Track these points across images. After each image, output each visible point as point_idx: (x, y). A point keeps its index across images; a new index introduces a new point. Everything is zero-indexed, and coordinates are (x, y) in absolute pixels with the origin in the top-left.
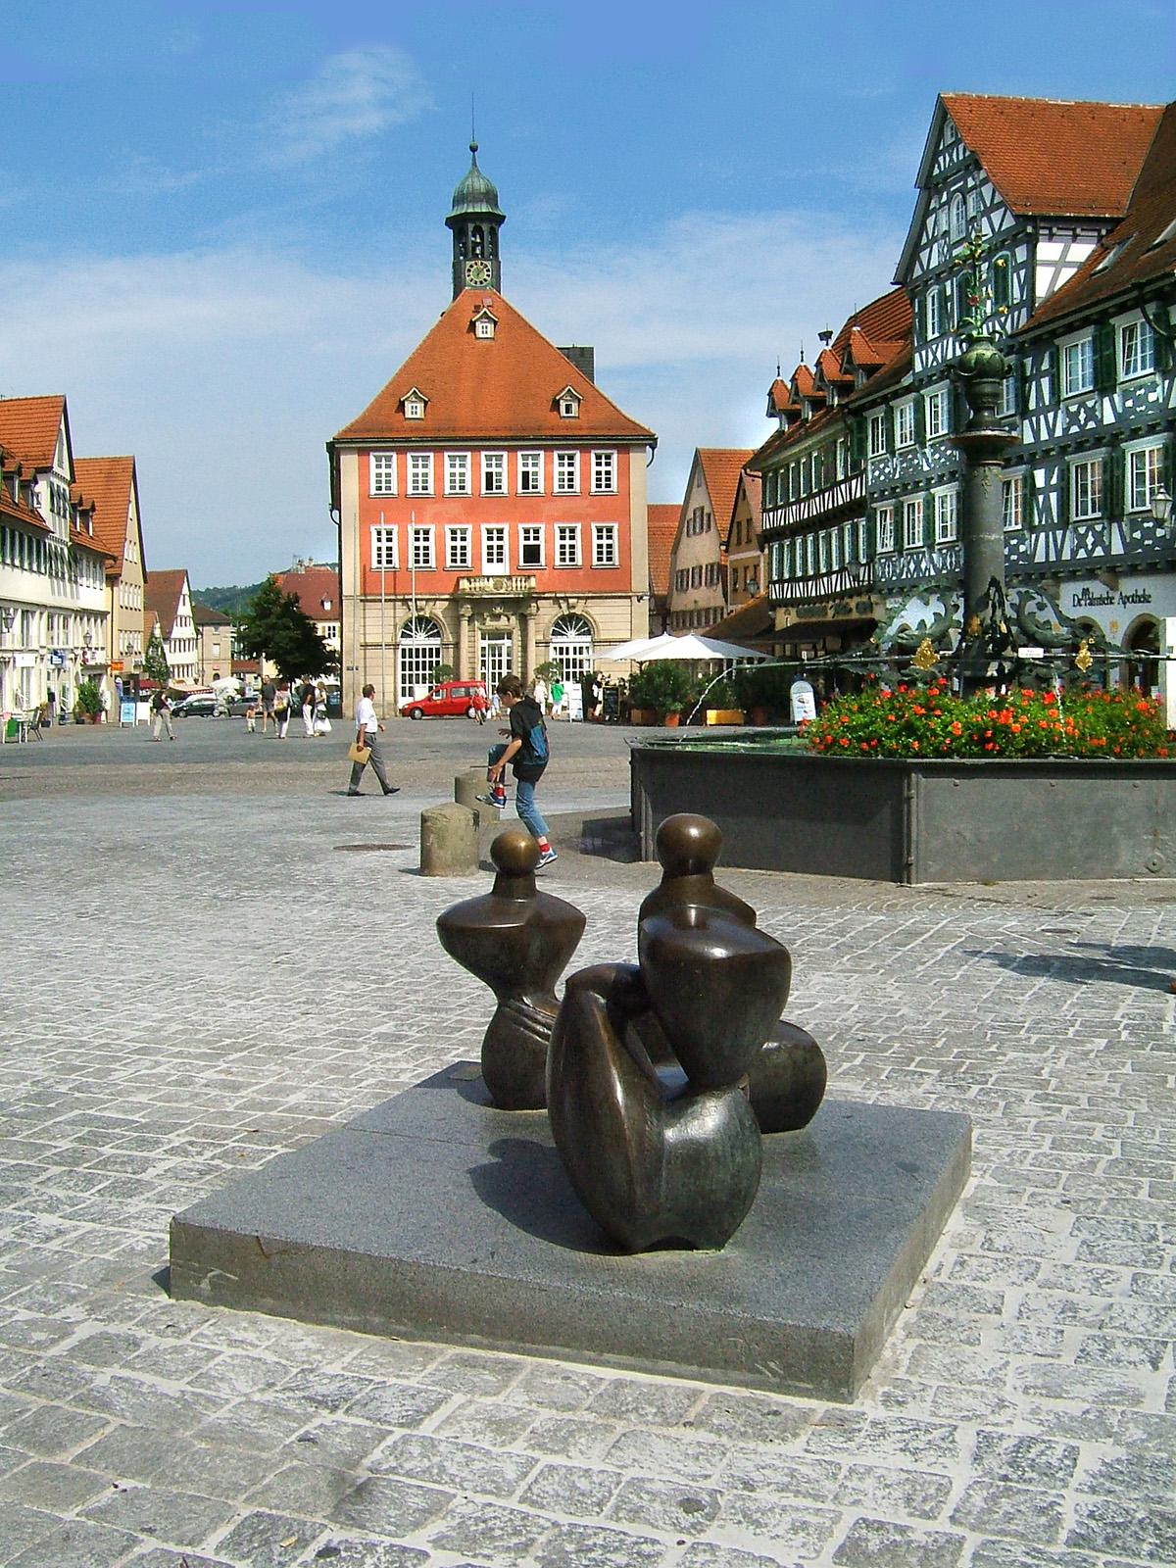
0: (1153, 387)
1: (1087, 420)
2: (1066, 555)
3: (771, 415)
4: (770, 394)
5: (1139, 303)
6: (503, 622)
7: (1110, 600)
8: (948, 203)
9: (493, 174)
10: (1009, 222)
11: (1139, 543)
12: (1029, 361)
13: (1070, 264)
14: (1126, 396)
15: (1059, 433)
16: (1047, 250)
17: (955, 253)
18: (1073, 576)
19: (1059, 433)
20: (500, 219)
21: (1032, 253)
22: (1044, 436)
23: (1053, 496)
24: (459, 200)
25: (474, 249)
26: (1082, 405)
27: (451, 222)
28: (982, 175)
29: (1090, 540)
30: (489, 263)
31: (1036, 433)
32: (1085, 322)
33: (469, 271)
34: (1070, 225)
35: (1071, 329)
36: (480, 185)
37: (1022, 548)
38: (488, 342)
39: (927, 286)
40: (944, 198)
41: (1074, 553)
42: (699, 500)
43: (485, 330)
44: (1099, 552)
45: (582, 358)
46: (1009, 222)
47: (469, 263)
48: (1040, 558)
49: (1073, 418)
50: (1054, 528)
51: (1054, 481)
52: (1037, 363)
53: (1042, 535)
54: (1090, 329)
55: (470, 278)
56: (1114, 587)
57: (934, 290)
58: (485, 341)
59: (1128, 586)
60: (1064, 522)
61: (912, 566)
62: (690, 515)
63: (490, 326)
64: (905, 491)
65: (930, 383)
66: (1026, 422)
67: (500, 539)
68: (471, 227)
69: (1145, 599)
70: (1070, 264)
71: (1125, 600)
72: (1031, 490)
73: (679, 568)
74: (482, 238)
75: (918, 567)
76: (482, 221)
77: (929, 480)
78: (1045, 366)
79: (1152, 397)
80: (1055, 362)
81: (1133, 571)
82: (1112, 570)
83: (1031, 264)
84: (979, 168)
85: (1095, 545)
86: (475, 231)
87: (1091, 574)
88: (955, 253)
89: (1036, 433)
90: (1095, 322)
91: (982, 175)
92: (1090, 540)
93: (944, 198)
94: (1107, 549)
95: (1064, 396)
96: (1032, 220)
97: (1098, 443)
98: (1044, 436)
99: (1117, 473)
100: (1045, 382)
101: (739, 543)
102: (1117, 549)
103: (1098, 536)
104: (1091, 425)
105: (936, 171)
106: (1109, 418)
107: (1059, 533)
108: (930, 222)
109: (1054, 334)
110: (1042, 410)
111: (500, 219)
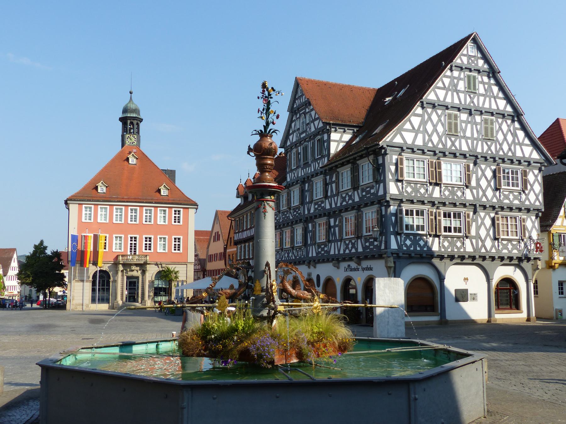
0: (372, 187)
1: (349, 200)
2: (342, 252)
3: (238, 197)
4: (237, 189)
5: (367, 155)
6: (135, 274)
7: (358, 269)
8: (299, 118)
9: (138, 103)
10: (321, 125)
11: (368, 247)
12: (328, 177)
13: (343, 142)
14: (363, 190)
15: (339, 205)
16: (335, 136)
17: (302, 136)
18: (344, 260)
19: (339, 205)
20: (141, 120)
21: (329, 136)
22: (333, 206)
23: (337, 229)
24: (125, 111)
25: (130, 130)
26: (347, 194)
27: (121, 119)
28: (311, 107)
29: (350, 246)
30: (136, 136)
31: (331, 205)
32: (348, 162)
34: (344, 126)
35: (343, 165)
36: (132, 106)
37: (326, 249)
39: (292, 149)
40: (298, 116)
41: (344, 251)
42: (217, 229)
43: (132, 161)
44: (353, 251)
45: (171, 174)
46: (321, 125)
47: (127, 136)
48: (332, 252)
49: (344, 199)
50: (336, 241)
51: (337, 223)
52: (331, 178)
53: (333, 244)
54: (350, 165)
55: (128, 142)
56: (359, 264)
57: (294, 150)
58: (132, 166)
59: (365, 264)
60: (341, 240)
61: (286, 255)
62: (214, 234)
63: (135, 160)
64: (284, 226)
65: (293, 185)
66: (327, 201)
67: (135, 241)
69: (370, 269)
70: (343, 142)
71: (363, 269)
72: (330, 227)
73: (210, 254)
74: (133, 126)
75: (288, 256)
77: (292, 222)
78: (334, 179)
79: (372, 191)
80: (337, 178)
81: (366, 258)
82: (358, 258)
83: (329, 140)
84: (310, 104)
85: (352, 248)
86: (130, 122)
87: (351, 259)
88: (302, 136)
89: (331, 205)
90: (352, 163)
91: (311, 107)
92: (350, 246)
93: (298, 116)
94: (356, 249)
95: (341, 190)
96: (329, 124)
97: (353, 208)
98: (333, 206)
99: (360, 220)
100: (334, 185)
101: (231, 245)
102: (360, 249)
103: (353, 245)
104: (350, 202)
105: (295, 106)
106: (357, 199)
107: (339, 243)
108: (293, 125)
109: (337, 167)
110: (333, 196)
111: (141, 120)
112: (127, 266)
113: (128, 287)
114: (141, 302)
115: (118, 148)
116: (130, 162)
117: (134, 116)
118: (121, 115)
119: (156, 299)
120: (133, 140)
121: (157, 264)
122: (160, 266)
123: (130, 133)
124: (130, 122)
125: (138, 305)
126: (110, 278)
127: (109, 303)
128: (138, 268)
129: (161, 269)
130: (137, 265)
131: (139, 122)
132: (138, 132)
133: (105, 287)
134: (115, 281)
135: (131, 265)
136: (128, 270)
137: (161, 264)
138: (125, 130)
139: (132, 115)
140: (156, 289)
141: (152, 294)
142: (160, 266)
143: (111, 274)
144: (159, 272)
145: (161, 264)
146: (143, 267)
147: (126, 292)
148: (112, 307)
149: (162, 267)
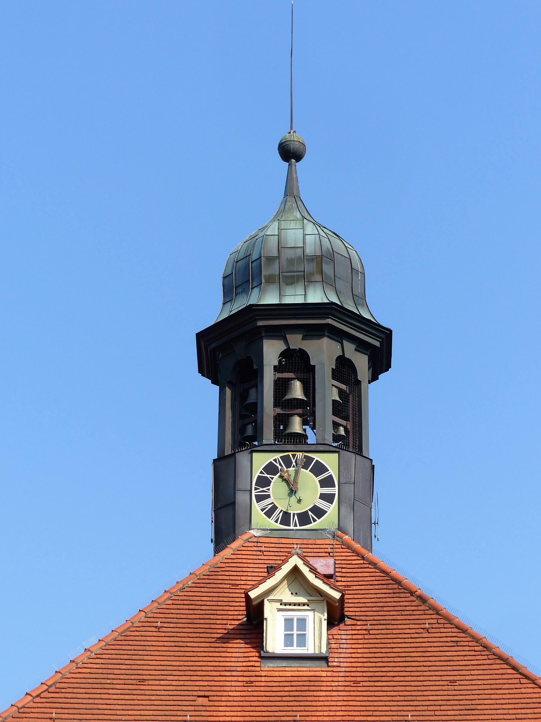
24: (243, 275)
25: (282, 421)
30: (330, 461)
33: (263, 482)
36: (300, 235)
38: (306, 668)
43: (292, 627)
47: (260, 461)
58: (292, 669)
68: (272, 351)
74: (309, 388)
76: (313, 332)
86: (285, 362)
115: (192, 549)
116: (275, 640)
117: (316, 296)
118: (212, 311)
120: (310, 489)
123: (286, 438)
124: (285, 362)
131: (361, 362)
132: (351, 440)
138: (242, 430)
139: (294, 296)
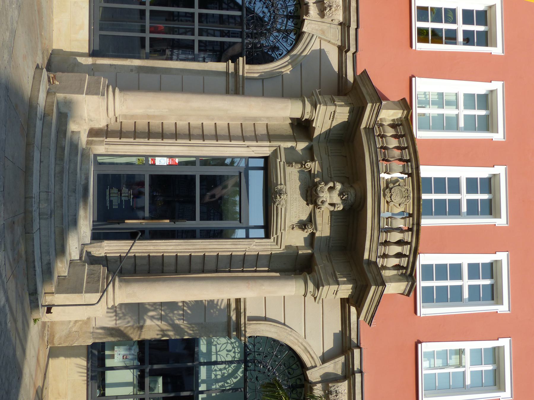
6: (293, 207)
112: (344, 154)
113: (198, 171)
114: (93, 260)
119: (118, 357)
121: (345, 345)
122: (335, 366)
125: (80, 238)
126: (250, 62)
127: (93, 54)
128: (324, 229)
129: (313, 375)
130: (351, 219)
133: (196, 38)
134: (236, 87)
135: (351, 175)
136: (314, 166)
137: (348, 374)
140: (191, 345)
141: (152, 329)
142: (335, 366)
143: (281, 65)
144: (295, 363)
145: (348, 374)
146: (343, 256)
147: (164, 156)
148: (58, 64)
149: (328, 380)
